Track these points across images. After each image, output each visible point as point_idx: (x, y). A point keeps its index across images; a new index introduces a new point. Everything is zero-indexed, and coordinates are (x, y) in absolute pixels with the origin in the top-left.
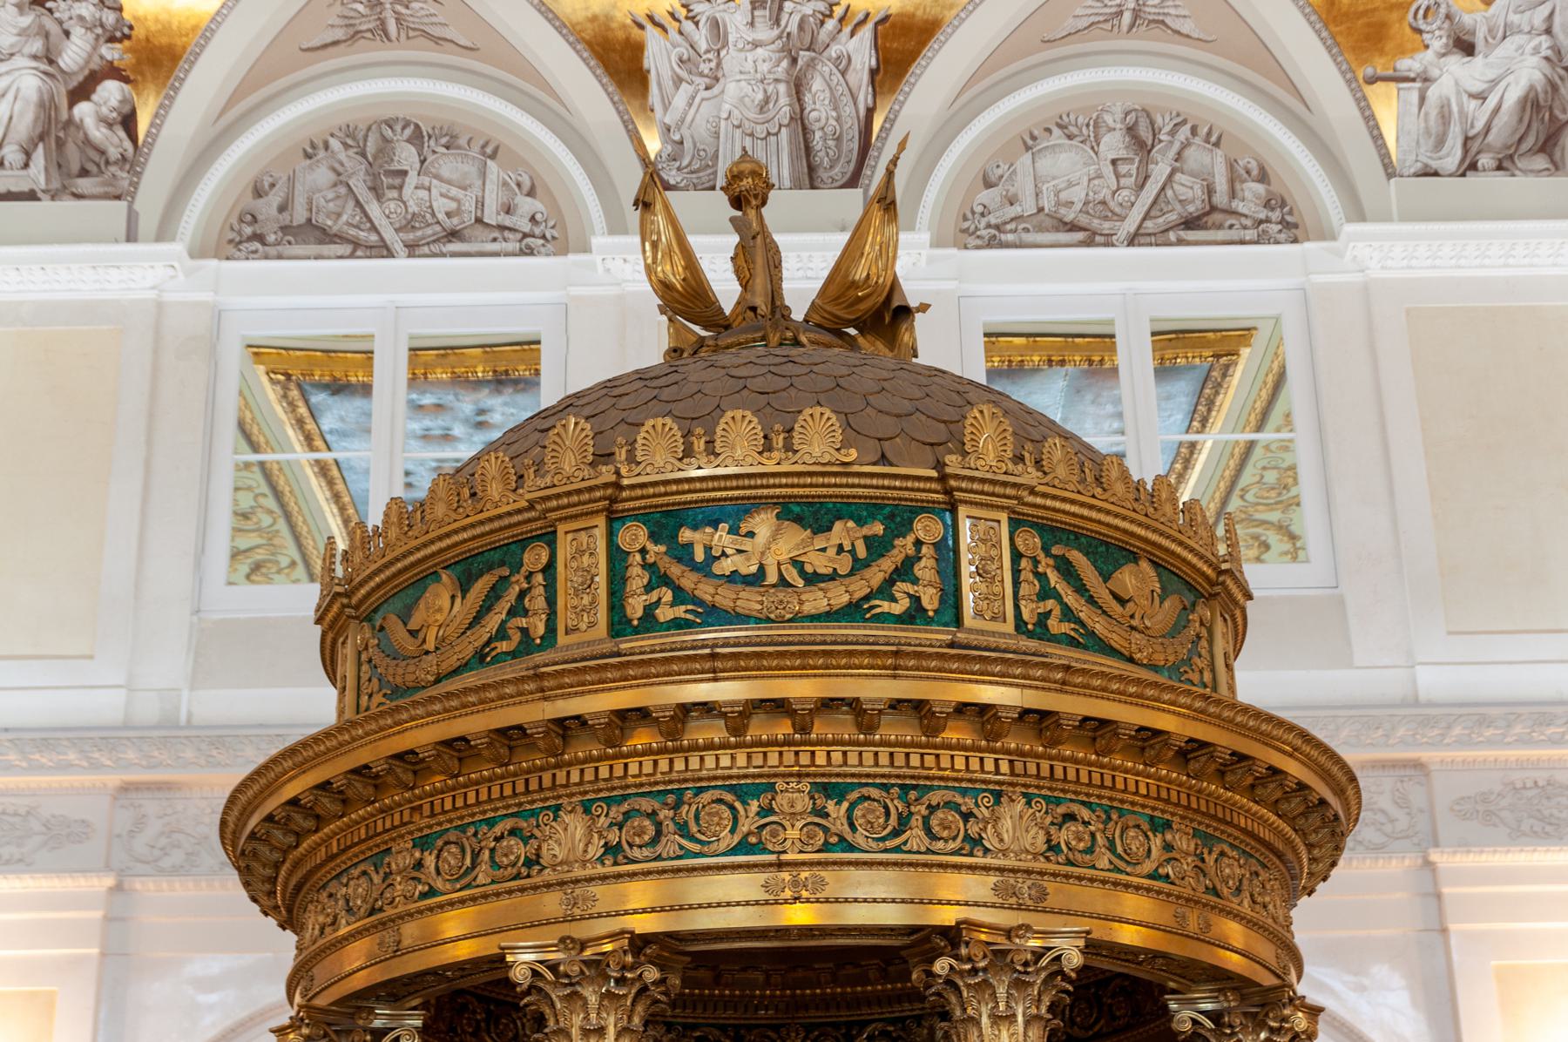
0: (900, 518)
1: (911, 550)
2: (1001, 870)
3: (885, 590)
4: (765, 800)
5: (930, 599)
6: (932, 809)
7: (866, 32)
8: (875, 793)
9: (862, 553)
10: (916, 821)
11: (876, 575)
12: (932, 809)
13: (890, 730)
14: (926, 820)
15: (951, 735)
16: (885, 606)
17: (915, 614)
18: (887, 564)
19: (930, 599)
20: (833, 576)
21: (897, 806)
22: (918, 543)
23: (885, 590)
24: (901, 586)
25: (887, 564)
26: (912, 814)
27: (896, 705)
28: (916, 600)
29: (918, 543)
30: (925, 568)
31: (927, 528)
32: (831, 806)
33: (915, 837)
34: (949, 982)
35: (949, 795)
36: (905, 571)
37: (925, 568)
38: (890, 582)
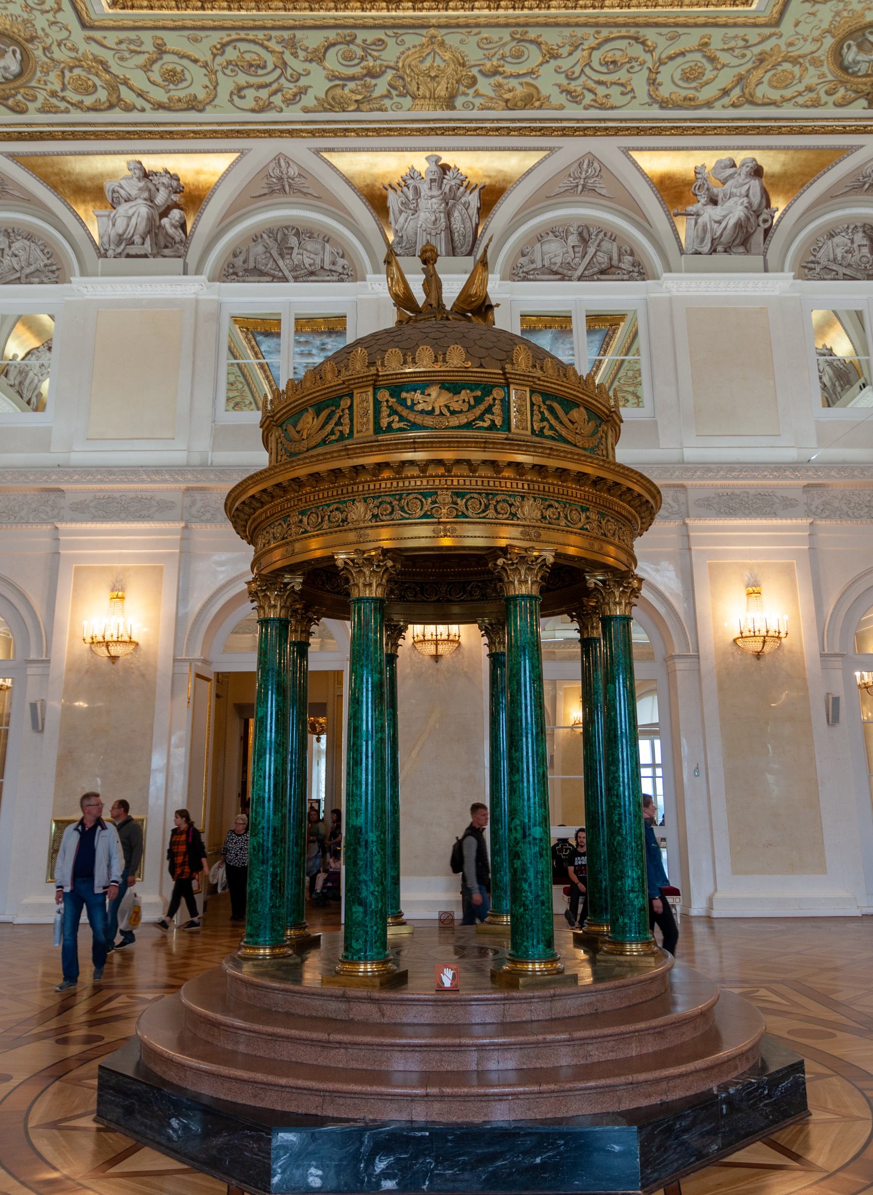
0: (487, 389)
1: (491, 402)
2: (523, 526)
3: (481, 418)
4: (434, 498)
5: (498, 421)
6: (498, 502)
7: (476, 193)
8: (476, 496)
9: (472, 403)
10: (492, 507)
11: (478, 411)
12: (498, 502)
13: (482, 472)
14: (495, 506)
15: (506, 474)
16: (481, 424)
17: (493, 427)
18: (482, 407)
19: (498, 421)
20: (461, 412)
21: (484, 501)
22: (494, 399)
23: (481, 418)
24: (487, 415)
25: (482, 407)
26: (492, 505)
27: (484, 462)
28: (493, 421)
29: (494, 399)
30: (497, 409)
31: (498, 393)
32: (459, 501)
33: (491, 513)
34: (503, 568)
35: (504, 497)
36: (489, 410)
37: (497, 409)
38: (483, 414)
